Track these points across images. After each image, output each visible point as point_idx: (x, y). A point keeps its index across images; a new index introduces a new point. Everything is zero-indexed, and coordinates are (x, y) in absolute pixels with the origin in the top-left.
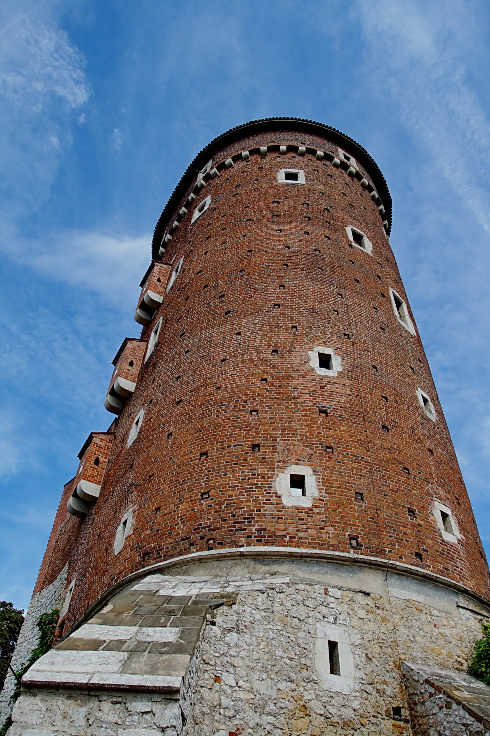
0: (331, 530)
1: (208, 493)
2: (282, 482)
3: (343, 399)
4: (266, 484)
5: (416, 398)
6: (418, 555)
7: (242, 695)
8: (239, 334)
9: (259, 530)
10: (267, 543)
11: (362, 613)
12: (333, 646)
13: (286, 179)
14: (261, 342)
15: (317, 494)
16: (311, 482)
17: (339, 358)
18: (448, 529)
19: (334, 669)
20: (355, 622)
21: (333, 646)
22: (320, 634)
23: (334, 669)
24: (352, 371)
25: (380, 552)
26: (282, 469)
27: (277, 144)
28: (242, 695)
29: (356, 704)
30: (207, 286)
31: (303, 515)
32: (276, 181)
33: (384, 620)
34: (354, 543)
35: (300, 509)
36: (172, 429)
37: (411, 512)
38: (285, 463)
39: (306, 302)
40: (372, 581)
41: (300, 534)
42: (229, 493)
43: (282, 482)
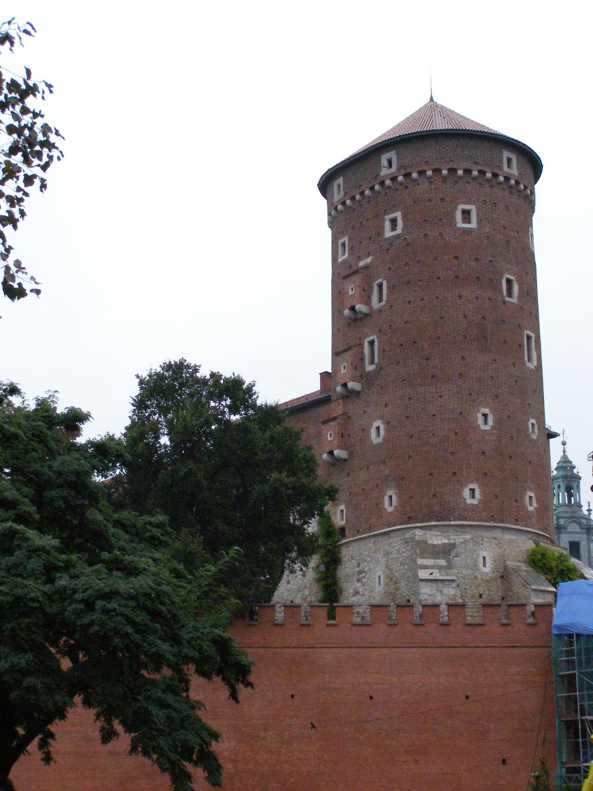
0: (484, 513)
1: (435, 495)
2: (466, 493)
3: (492, 444)
4: (460, 494)
5: (528, 427)
6: (517, 520)
7: (460, 575)
8: (441, 396)
9: (458, 515)
10: (461, 520)
11: (494, 546)
12: (484, 558)
13: (463, 223)
14: (453, 406)
15: (479, 496)
16: (477, 492)
17: (492, 416)
18: (531, 504)
19: (484, 565)
20: (492, 550)
21: (484, 558)
22: (480, 554)
23: (484, 565)
24: (498, 422)
25: (502, 521)
26: (466, 486)
27: (455, 166)
28: (460, 575)
29: (490, 575)
30: (415, 342)
31: (474, 508)
32: (456, 224)
33: (501, 547)
34: (493, 518)
35: (473, 505)
36: (410, 454)
37: (516, 500)
38: (467, 483)
39: (476, 372)
40: (498, 534)
41: (474, 516)
42: (444, 497)
43: (466, 493)
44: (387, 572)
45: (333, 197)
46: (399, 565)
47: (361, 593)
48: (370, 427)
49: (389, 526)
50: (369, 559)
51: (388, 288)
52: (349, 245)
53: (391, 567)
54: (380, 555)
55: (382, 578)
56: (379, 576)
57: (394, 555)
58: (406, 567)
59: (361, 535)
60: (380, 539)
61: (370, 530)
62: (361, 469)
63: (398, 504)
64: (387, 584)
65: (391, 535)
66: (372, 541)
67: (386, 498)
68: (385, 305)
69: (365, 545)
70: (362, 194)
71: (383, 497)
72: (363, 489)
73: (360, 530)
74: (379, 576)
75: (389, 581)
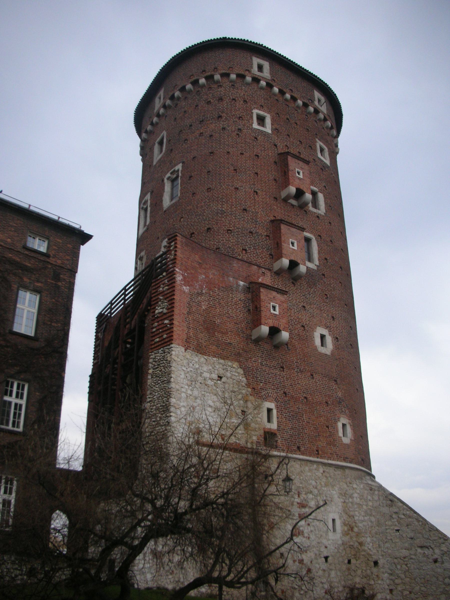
44: (345, 517)
45: (252, 67)
46: (363, 513)
47: (306, 535)
48: (313, 330)
49: (345, 460)
50: (316, 491)
51: (326, 203)
52: (272, 124)
53: (351, 513)
54: (335, 493)
55: (338, 523)
56: (334, 520)
57: (355, 499)
58: (373, 519)
59: (303, 454)
60: (331, 470)
61: (317, 453)
62: (301, 371)
63: (353, 439)
64: (345, 534)
65: (347, 471)
66: (321, 470)
67: (340, 425)
68: (323, 216)
69: (310, 470)
70: (294, 99)
71: (336, 423)
72: (305, 398)
73: (302, 449)
74: (334, 520)
75: (349, 530)
